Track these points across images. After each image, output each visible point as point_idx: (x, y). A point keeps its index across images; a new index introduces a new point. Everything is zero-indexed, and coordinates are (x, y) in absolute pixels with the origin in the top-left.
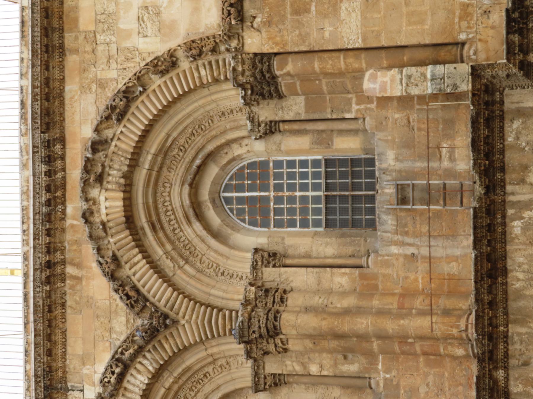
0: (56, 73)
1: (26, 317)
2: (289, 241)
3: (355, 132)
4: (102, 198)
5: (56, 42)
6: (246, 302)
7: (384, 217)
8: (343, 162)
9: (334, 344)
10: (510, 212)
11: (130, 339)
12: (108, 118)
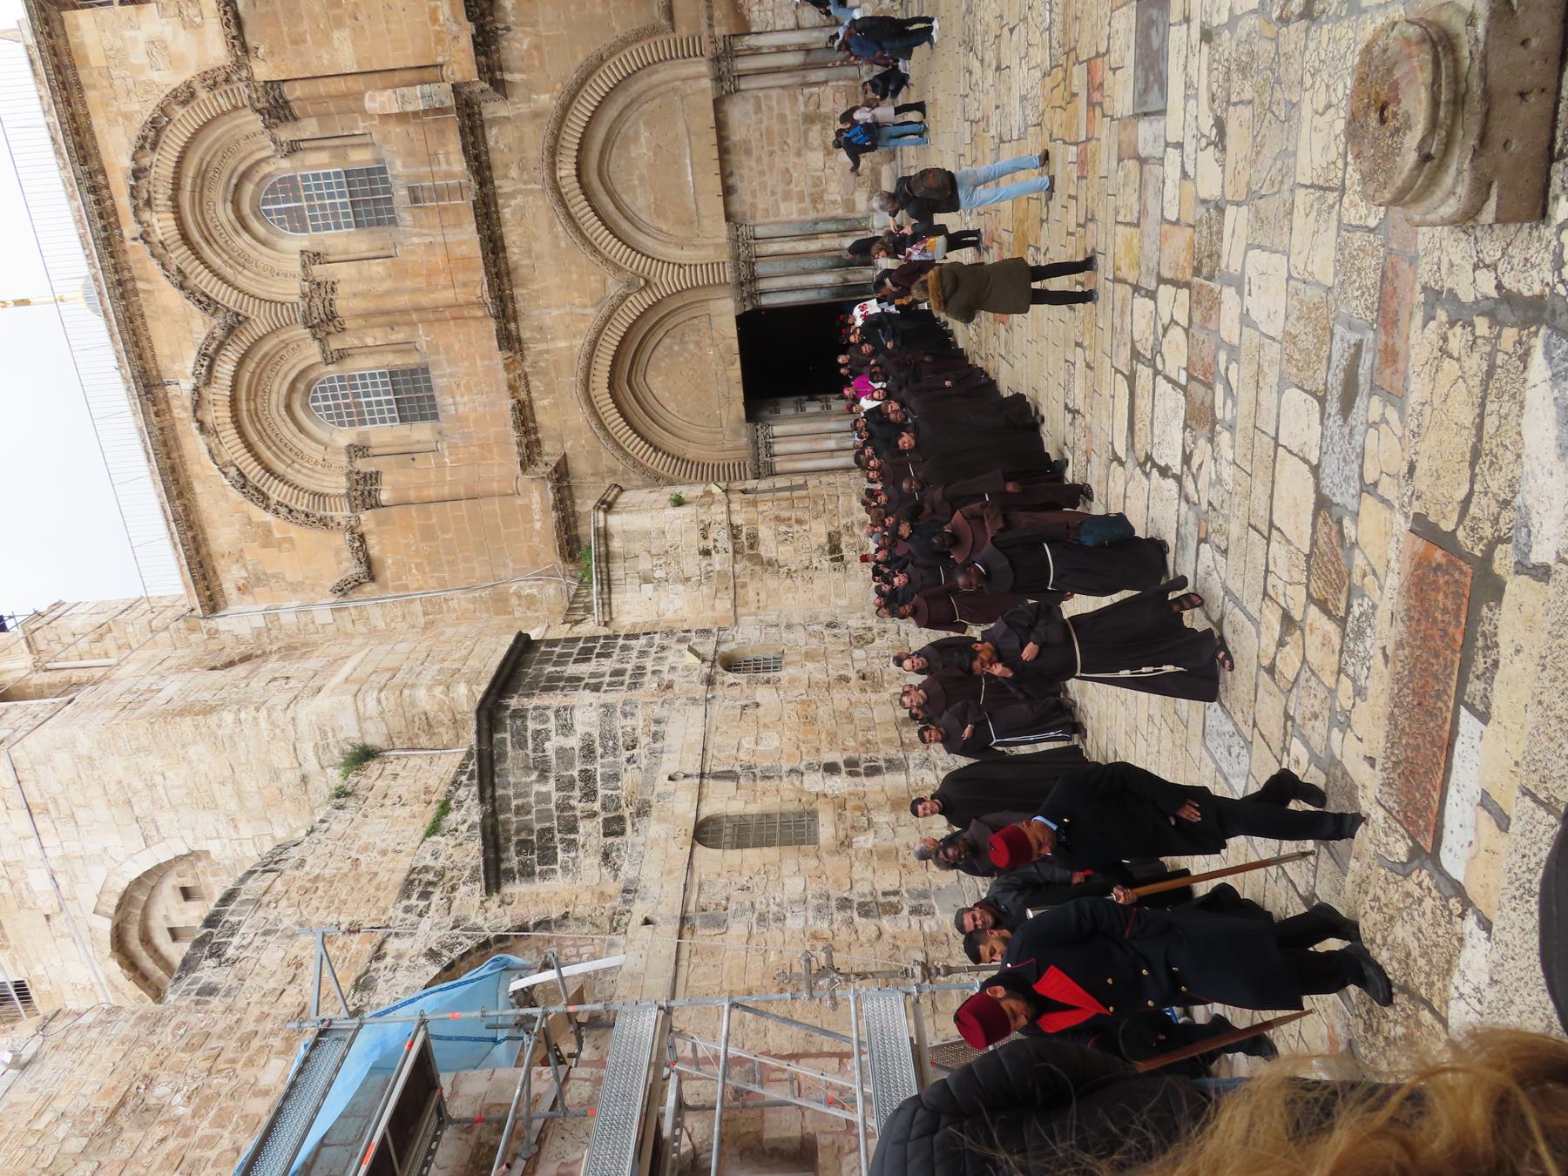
0: (80, 110)
1: (110, 330)
2: (328, 242)
3: (366, 145)
4: (154, 220)
5: (72, 79)
6: (304, 295)
7: (403, 215)
8: (359, 172)
9: (381, 320)
10: (500, 201)
11: (211, 336)
12: (142, 147)
